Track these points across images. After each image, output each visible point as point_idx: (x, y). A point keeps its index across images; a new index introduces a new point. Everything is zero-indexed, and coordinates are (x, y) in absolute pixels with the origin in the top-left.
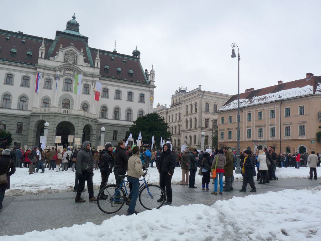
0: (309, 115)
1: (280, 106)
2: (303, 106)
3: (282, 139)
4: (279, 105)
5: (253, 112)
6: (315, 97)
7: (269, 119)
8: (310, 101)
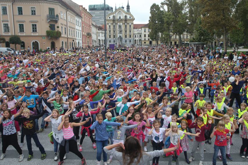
0: (40, 16)
1: (12, 4)
2: (35, 8)
3: (16, 35)
4: (12, 3)
6: (45, 2)
7: (1, 15)
8: (40, 4)
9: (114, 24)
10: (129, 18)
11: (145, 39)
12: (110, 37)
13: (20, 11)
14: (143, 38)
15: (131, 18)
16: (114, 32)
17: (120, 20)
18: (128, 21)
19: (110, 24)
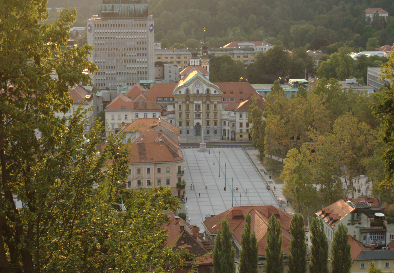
5: (133, 168)
9: (188, 102)
10: (214, 93)
11: (241, 131)
12: (180, 125)
13: (159, 170)
14: (238, 130)
15: (217, 93)
16: (188, 116)
17: (198, 96)
18: (211, 98)
19: (180, 103)
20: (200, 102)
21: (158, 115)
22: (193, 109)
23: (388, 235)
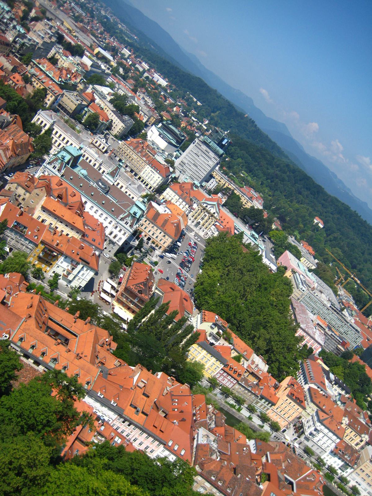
20: (207, 215)
21: (187, 206)
22: (202, 215)
23: (219, 342)
